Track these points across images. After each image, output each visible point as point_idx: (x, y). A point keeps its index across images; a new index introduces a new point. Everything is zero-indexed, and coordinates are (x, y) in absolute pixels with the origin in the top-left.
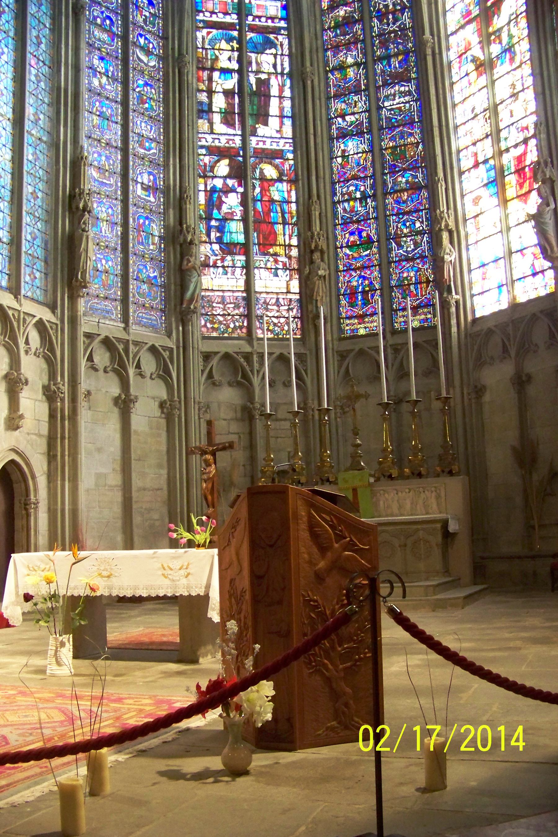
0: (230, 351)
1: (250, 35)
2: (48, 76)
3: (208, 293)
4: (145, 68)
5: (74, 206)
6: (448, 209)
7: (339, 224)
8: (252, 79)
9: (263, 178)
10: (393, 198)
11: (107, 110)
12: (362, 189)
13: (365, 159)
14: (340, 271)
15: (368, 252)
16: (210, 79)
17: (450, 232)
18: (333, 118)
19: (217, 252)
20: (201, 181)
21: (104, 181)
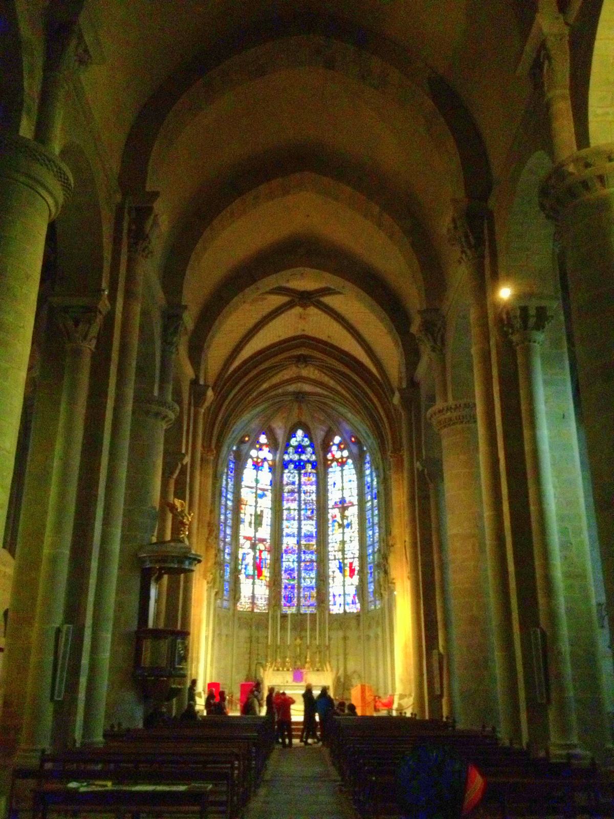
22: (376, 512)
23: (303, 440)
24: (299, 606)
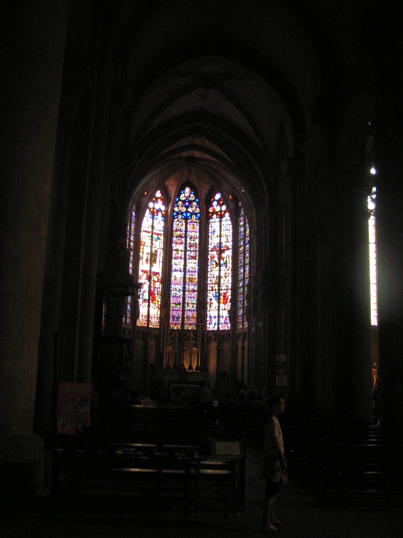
9: (154, 281)
22: (248, 255)
23: (190, 196)
24: (183, 324)
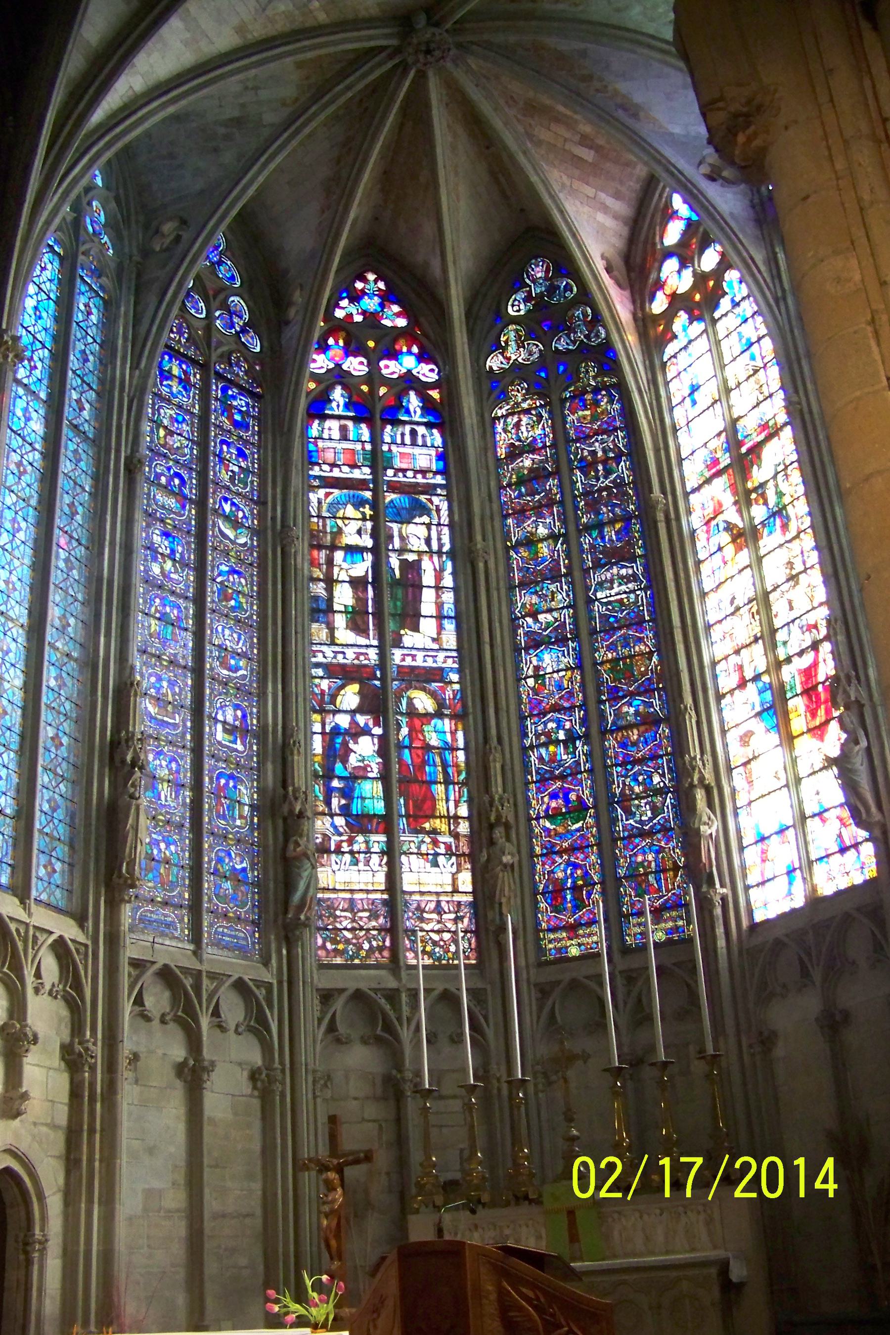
0: (364, 986)
1: (390, 497)
2: (83, 560)
3: (327, 895)
4: (231, 546)
5: (117, 759)
6: (702, 753)
7: (533, 782)
8: (394, 562)
9: (412, 713)
10: (616, 739)
11: (172, 611)
12: (568, 725)
13: (570, 680)
14: (537, 856)
15: (580, 824)
16: (330, 562)
17: (708, 790)
18: (519, 618)
19: (341, 830)
20: (316, 717)
21: (166, 719)
